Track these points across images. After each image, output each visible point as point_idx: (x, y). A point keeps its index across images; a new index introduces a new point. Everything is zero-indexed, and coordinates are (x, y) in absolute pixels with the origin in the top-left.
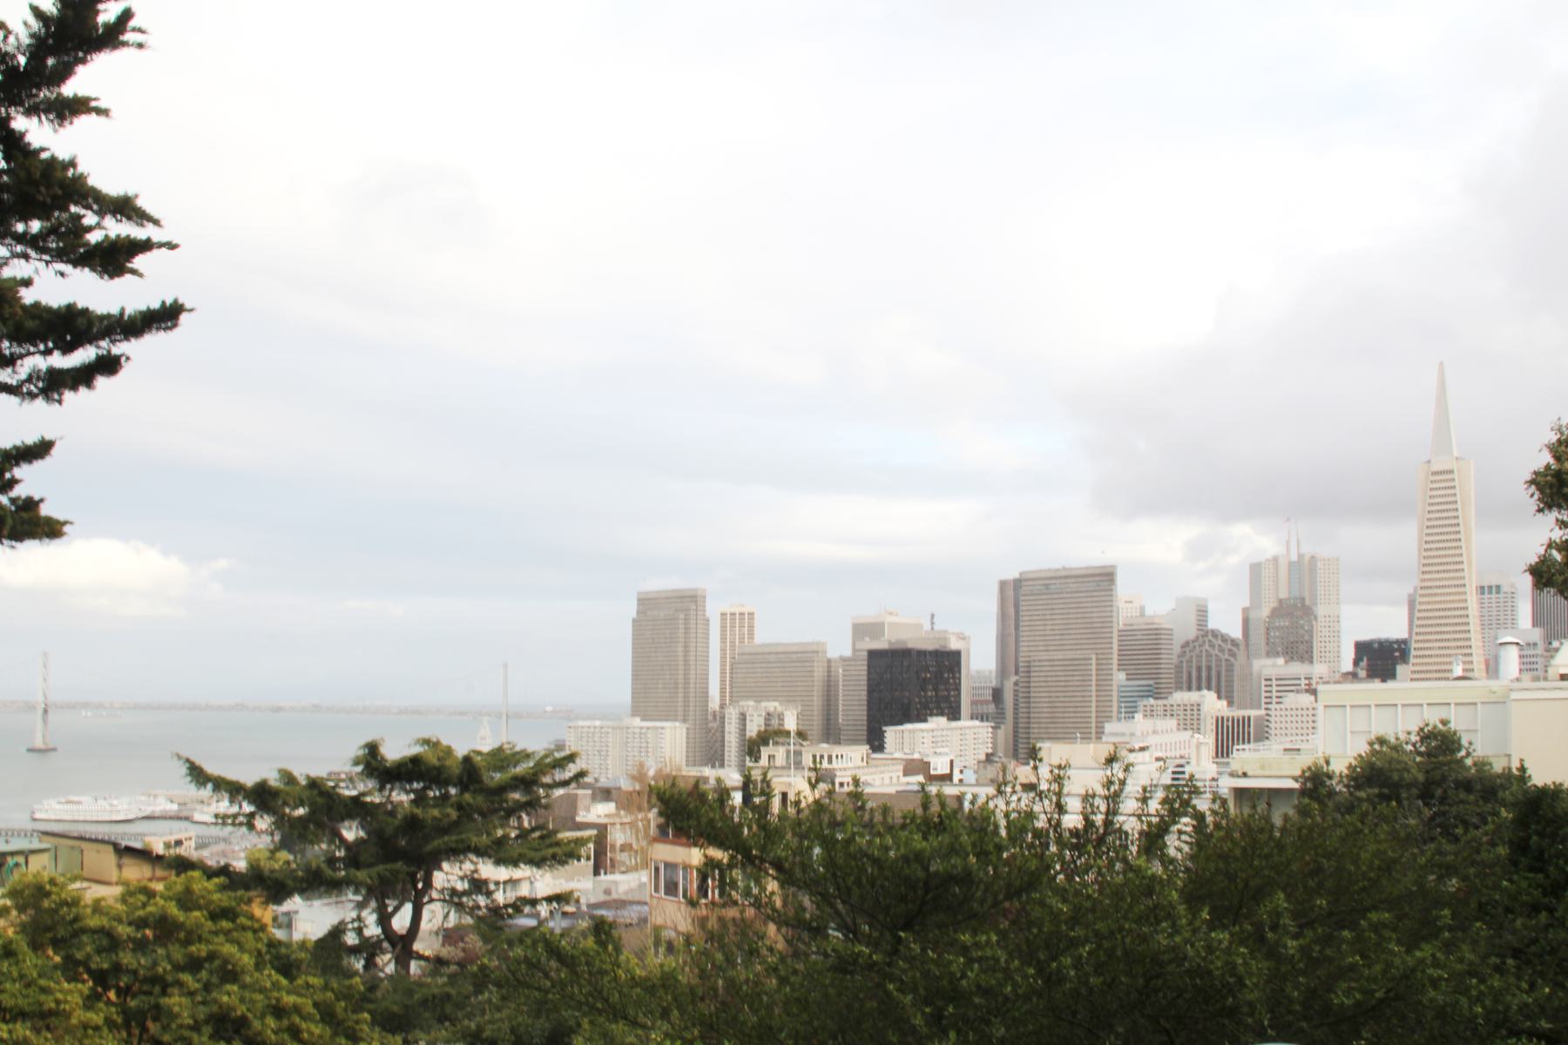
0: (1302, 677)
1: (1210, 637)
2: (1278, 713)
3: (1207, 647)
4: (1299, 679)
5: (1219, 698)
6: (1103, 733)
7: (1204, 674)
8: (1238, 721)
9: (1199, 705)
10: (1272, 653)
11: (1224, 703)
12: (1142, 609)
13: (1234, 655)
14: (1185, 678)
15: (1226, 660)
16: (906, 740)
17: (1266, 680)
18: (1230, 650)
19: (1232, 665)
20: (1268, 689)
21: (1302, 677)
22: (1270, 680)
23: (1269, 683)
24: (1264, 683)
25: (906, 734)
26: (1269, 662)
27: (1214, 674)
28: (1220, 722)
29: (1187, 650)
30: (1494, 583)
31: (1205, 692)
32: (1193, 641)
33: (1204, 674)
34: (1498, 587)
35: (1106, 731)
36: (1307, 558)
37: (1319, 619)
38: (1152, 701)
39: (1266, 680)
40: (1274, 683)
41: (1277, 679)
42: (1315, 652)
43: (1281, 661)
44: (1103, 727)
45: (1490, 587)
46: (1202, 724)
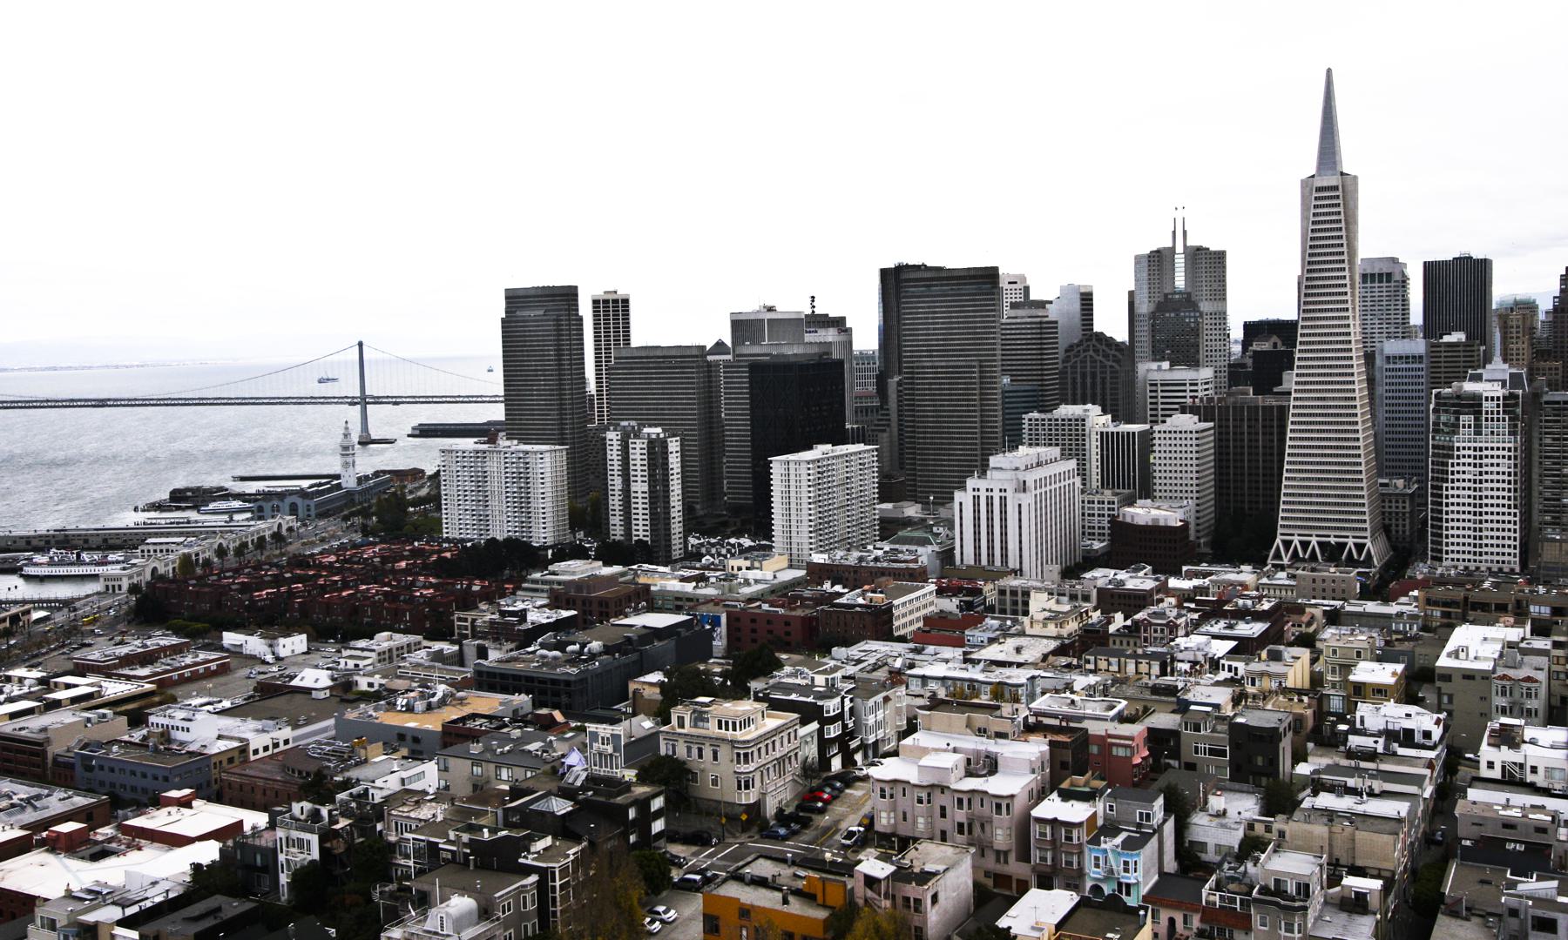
1: (1094, 342)
2: (1163, 442)
3: (1091, 353)
4: (1185, 385)
5: (1105, 412)
6: (988, 465)
7: (1089, 380)
9: (1084, 420)
10: (1157, 355)
11: (1109, 416)
12: (1027, 289)
14: (1069, 386)
15: (1111, 367)
16: (792, 472)
17: (1151, 385)
18: (1114, 356)
21: (1188, 382)
23: (1154, 388)
24: (1149, 388)
25: (792, 466)
26: (1154, 366)
27: (1098, 380)
28: (1104, 436)
29: (1071, 354)
30: (1385, 271)
31: (1089, 406)
32: (1078, 345)
33: (1089, 380)
34: (1389, 275)
35: (992, 465)
38: (1035, 415)
39: (1151, 385)
40: (1160, 388)
41: (1162, 385)
42: (1201, 352)
43: (1166, 365)
44: (988, 460)
45: (1381, 275)
46: (1087, 440)
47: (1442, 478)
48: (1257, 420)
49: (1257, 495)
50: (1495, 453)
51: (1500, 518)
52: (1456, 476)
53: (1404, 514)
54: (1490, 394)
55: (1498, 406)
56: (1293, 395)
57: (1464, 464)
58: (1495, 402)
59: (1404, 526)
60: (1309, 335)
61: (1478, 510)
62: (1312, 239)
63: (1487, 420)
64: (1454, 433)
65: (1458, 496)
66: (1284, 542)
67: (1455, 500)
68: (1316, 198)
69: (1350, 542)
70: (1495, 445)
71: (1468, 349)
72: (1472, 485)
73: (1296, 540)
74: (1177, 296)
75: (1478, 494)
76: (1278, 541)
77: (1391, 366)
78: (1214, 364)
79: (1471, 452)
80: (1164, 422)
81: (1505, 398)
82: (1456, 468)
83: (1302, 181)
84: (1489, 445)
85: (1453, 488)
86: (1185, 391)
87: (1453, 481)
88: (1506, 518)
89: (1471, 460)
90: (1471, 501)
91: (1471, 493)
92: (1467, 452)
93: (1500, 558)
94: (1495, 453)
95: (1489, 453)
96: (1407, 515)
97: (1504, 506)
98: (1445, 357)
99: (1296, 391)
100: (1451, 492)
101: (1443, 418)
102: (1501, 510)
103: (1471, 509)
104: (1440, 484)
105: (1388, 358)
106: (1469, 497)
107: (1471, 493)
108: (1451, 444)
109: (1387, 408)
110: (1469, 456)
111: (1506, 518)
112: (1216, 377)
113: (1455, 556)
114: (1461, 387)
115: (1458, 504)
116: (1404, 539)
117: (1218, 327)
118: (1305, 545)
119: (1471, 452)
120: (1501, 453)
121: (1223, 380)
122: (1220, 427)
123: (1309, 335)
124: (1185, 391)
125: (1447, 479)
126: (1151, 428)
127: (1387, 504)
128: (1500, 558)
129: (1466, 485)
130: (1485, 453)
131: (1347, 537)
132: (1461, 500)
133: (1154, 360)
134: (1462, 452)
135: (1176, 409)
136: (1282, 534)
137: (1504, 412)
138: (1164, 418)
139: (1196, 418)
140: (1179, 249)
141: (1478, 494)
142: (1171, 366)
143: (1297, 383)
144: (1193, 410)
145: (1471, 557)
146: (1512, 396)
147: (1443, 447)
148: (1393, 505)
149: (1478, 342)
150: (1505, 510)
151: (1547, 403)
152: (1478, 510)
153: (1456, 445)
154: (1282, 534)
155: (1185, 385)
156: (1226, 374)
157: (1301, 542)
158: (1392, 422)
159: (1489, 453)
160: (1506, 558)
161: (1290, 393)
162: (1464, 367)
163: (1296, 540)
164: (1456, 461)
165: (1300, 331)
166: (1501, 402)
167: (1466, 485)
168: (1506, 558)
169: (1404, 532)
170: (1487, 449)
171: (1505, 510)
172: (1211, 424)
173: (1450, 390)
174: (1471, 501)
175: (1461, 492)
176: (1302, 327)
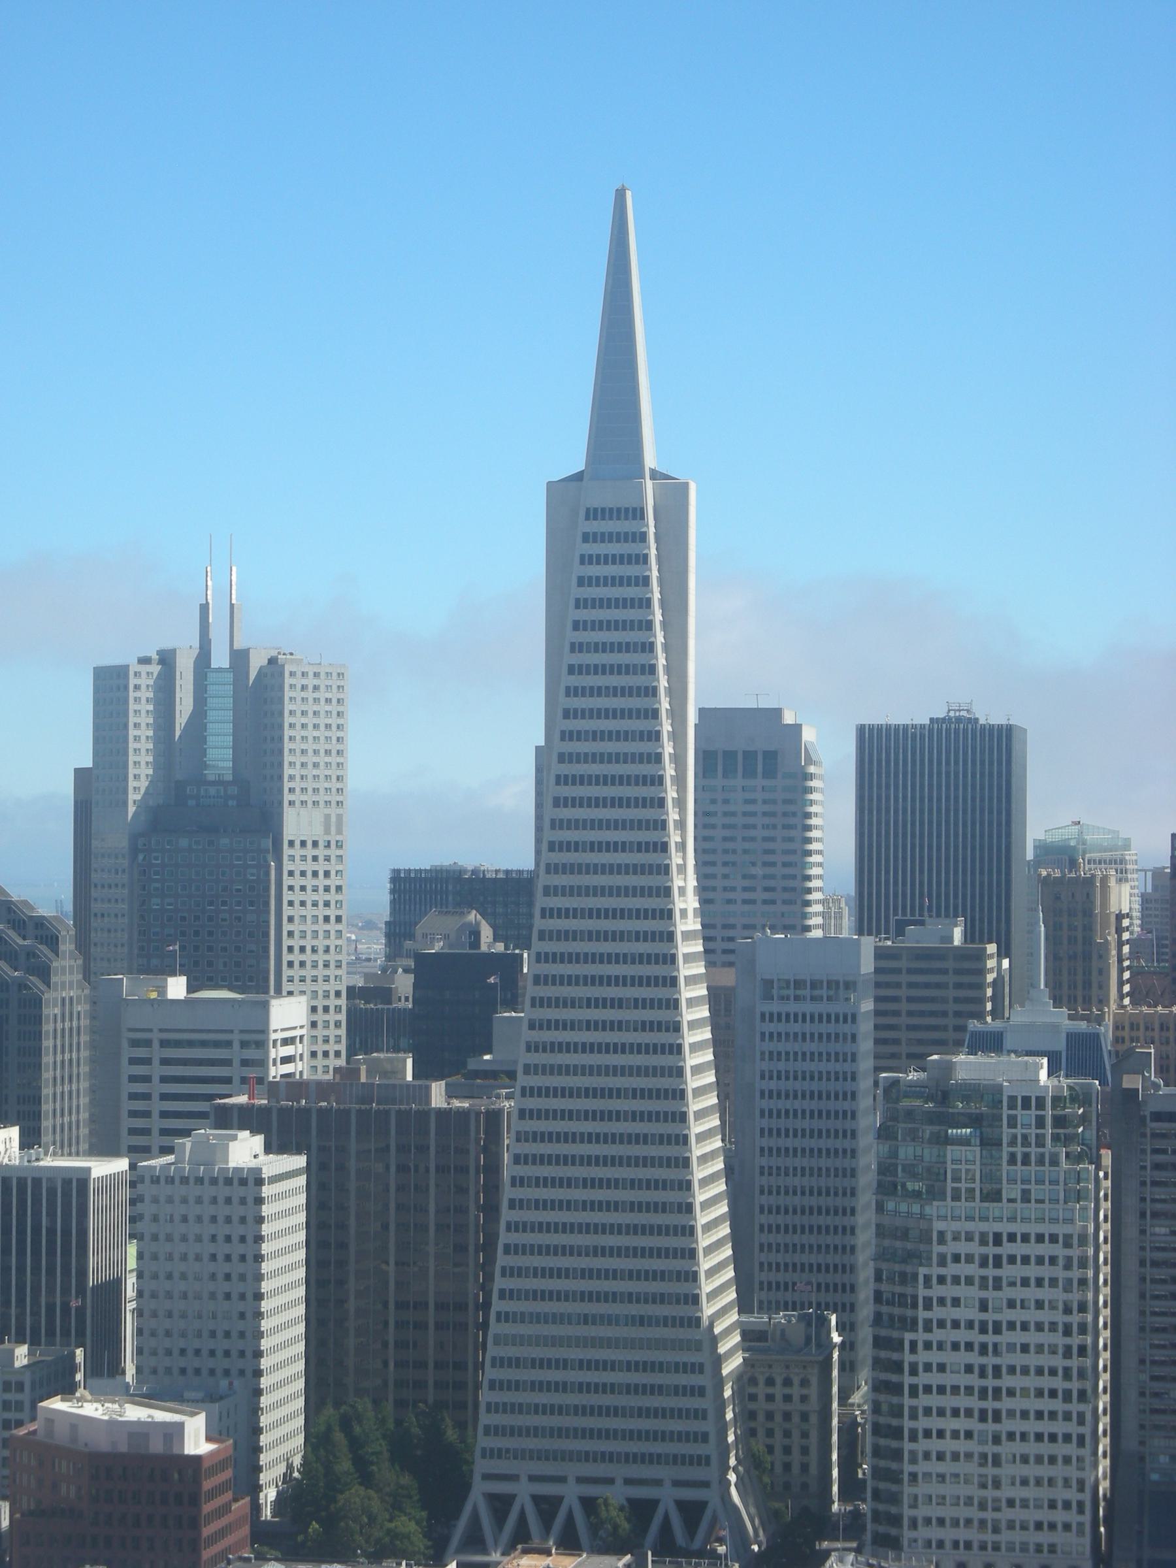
0: (236, 1038)
4: (228, 1044)
8: (52, 1192)
13: (44, 973)
17: (135, 1043)
19: (37, 1003)
20: (140, 1105)
21: (236, 1038)
22: (148, 1043)
23: (141, 1053)
24: (127, 1052)
36: (257, 662)
37: (287, 851)
39: (135, 1043)
41: (164, 1044)
43: (177, 987)
47: (902, 1319)
48: (423, 1149)
49: (421, 1365)
50: (1034, 1249)
51: (1045, 1427)
52: (937, 1313)
53: (805, 1417)
54: (1020, 1093)
55: (1040, 1122)
56: (522, 1080)
57: (956, 1280)
58: (1033, 1112)
59: (805, 1451)
60: (566, 913)
61: (990, 1404)
62: (576, 648)
63: (1012, 1160)
64: (936, 1194)
65: (942, 1368)
66: (492, 1498)
67: (934, 1379)
68: (586, 538)
69: (667, 1496)
70: (1033, 1229)
71: (967, 965)
72: (975, 1337)
73: (523, 1491)
74: (212, 791)
75: (990, 1360)
76: (479, 1490)
77: (775, 1007)
78: (309, 986)
79: (975, 1248)
80: (167, 1150)
81: (1057, 1100)
82: (937, 1291)
83: (550, 485)
84: (1018, 1228)
85: (928, 1346)
86: (227, 1063)
87: (928, 1328)
88: (1059, 1427)
89: (972, 1270)
90: (974, 1380)
91: (974, 1358)
92: (963, 1248)
93: (1044, 1537)
94: (1034, 1249)
95: (1018, 1249)
96: (814, 1419)
97: (1053, 1393)
98: (911, 985)
99: (527, 1069)
100: (923, 1357)
101: (906, 1152)
102: (1046, 1404)
103: (974, 1403)
104: (895, 1334)
105: (768, 984)
106: (969, 1369)
107: (974, 1358)
108: (923, 1225)
109: (765, 1123)
110: (969, 1259)
111: (1059, 1427)
112: (314, 1024)
113: (935, 1533)
114: (949, 1068)
115: (941, 1390)
116: (804, 1486)
117: (321, 881)
118: (547, 1507)
119: (975, 1248)
120: (1046, 1249)
121: (332, 1032)
122: (323, 1167)
123: (566, 913)
124: (227, 1063)
125: (914, 1321)
126: (133, 1166)
127: (761, 1390)
128: (1044, 1537)
129: (962, 1335)
130: (1007, 1249)
131: (658, 1483)
132: (948, 1379)
133: (146, 970)
134: (951, 1248)
135: (202, 1115)
136: (487, 1477)
137: (1056, 1138)
138: (166, 1141)
139: (258, 1141)
140: (220, 659)
141: (990, 1360)
142: (190, 989)
143: (531, 1047)
144: (249, 1119)
145: (973, 1535)
146: (1079, 1097)
147: (905, 1235)
148: (778, 1391)
149: (992, 948)
150: (1058, 1405)
151: (1158, 1117)
152: (990, 1404)
153: (938, 1226)
154: (487, 1477)
155: (228, 1044)
156: (342, 1017)
157: (537, 1499)
158: (775, 1161)
159: (1018, 1249)
160: (1058, 1537)
161: (512, 1075)
162: (958, 1014)
163: (523, 1491)
164: (936, 1271)
165: (541, 901)
166: (1049, 1113)
167: (962, 1335)
168: (1058, 1537)
169: (805, 1468)
170: (1012, 1238)
171: (1058, 1405)
172: (300, 1161)
173: (922, 1075)
174: (974, 1380)
175: (947, 1357)
176: (547, 891)
